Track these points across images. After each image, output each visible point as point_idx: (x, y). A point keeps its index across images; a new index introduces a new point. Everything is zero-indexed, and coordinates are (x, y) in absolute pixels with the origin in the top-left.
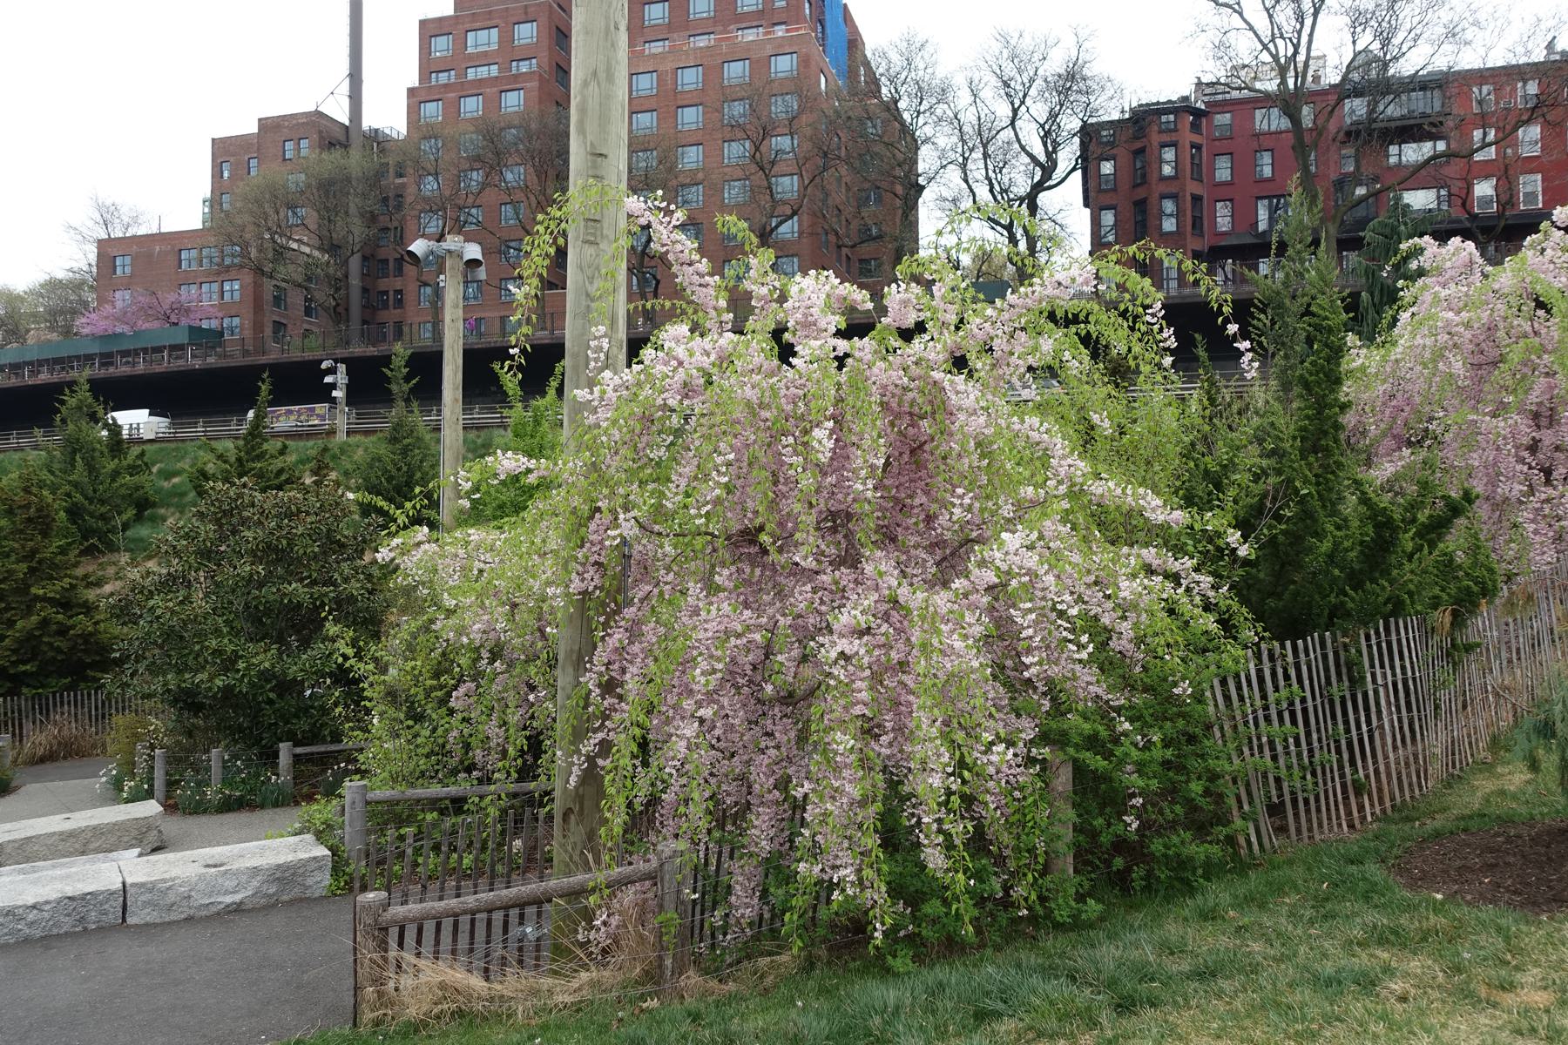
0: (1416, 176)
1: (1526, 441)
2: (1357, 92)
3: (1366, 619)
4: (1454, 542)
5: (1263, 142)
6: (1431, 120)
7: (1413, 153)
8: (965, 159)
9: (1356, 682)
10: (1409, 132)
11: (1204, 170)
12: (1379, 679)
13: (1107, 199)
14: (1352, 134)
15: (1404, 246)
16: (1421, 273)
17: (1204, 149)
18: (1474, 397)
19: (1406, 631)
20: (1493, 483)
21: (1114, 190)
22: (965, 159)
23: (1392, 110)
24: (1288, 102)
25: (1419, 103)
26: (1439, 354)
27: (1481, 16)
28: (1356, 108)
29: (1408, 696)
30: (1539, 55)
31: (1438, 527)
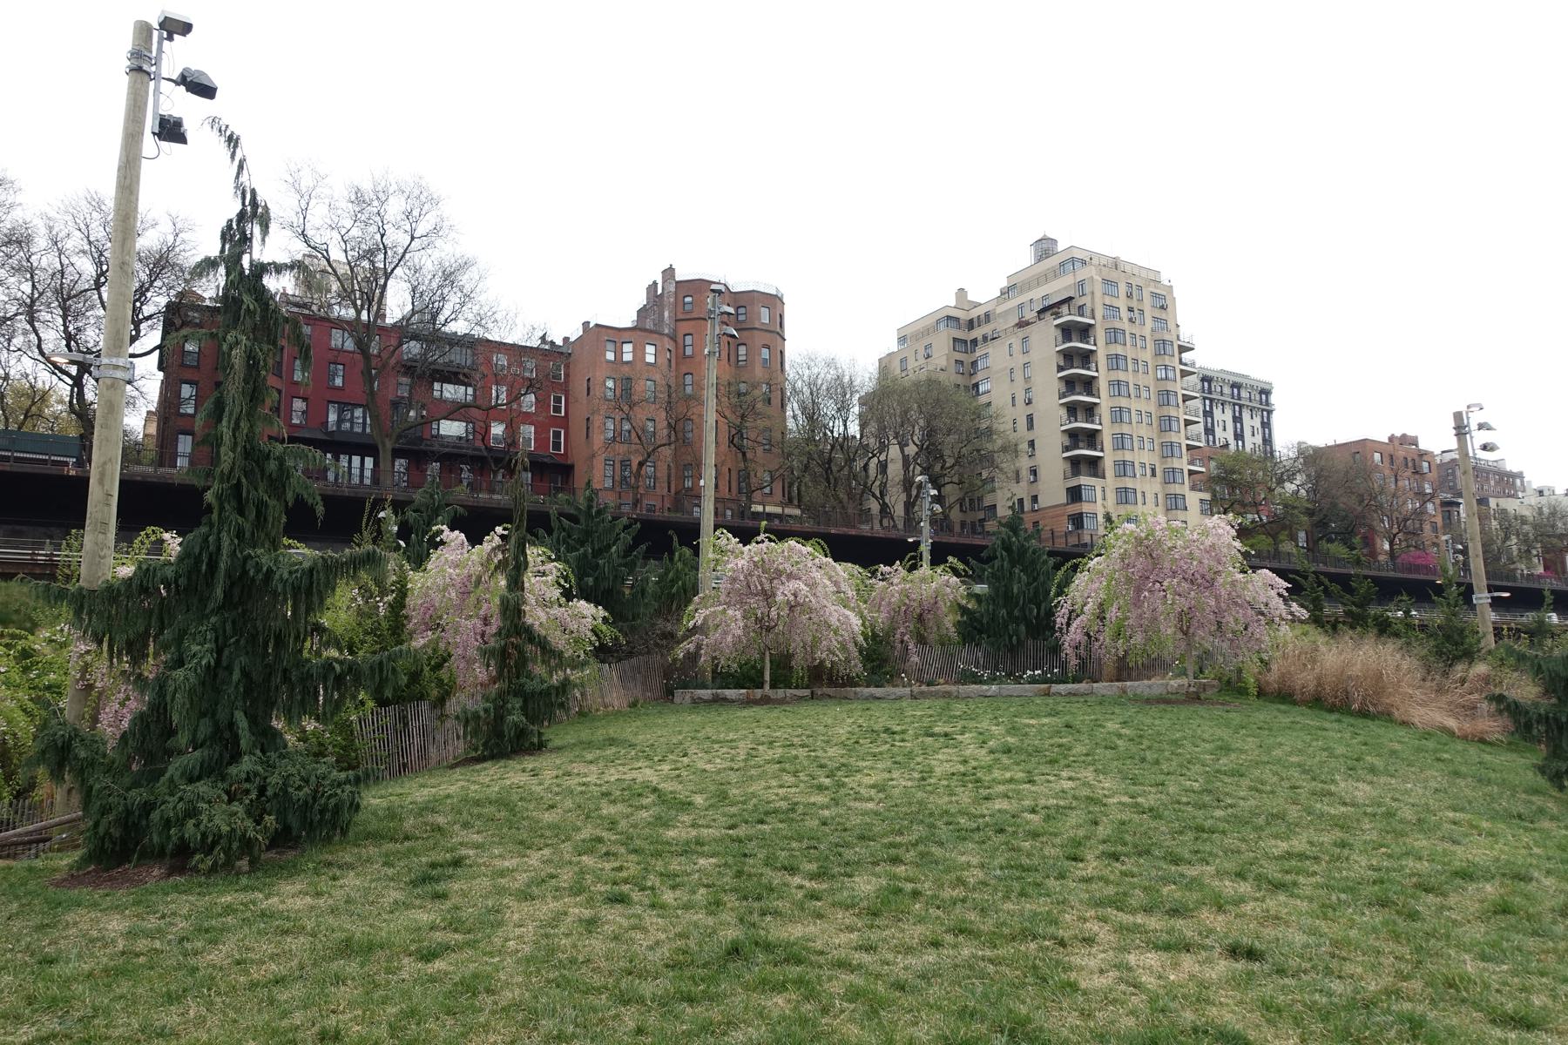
0: (455, 411)
1: (478, 631)
2: (415, 337)
3: (411, 700)
4: (444, 674)
5: (338, 355)
6: (466, 370)
7: (451, 392)
8: (33, 302)
9: (405, 725)
10: (453, 377)
11: (284, 369)
12: (414, 725)
13: (188, 375)
14: (409, 368)
15: (434, 528)
16: (442, 543)
17: (286, 351)
18: (460, 609)
19: (425, 706)
20: (465, 650)
21: (197, 367)
22: (33, 302)
23: (438, 357)
24: (364, 332)
25: (458, 357)
26: (445, 589)
27: (498, 316)
28: (413, 348)
29: (424, 732)
30: (535, 343)
31: (439, 666)
